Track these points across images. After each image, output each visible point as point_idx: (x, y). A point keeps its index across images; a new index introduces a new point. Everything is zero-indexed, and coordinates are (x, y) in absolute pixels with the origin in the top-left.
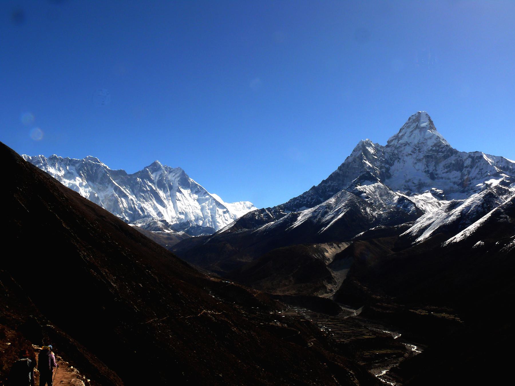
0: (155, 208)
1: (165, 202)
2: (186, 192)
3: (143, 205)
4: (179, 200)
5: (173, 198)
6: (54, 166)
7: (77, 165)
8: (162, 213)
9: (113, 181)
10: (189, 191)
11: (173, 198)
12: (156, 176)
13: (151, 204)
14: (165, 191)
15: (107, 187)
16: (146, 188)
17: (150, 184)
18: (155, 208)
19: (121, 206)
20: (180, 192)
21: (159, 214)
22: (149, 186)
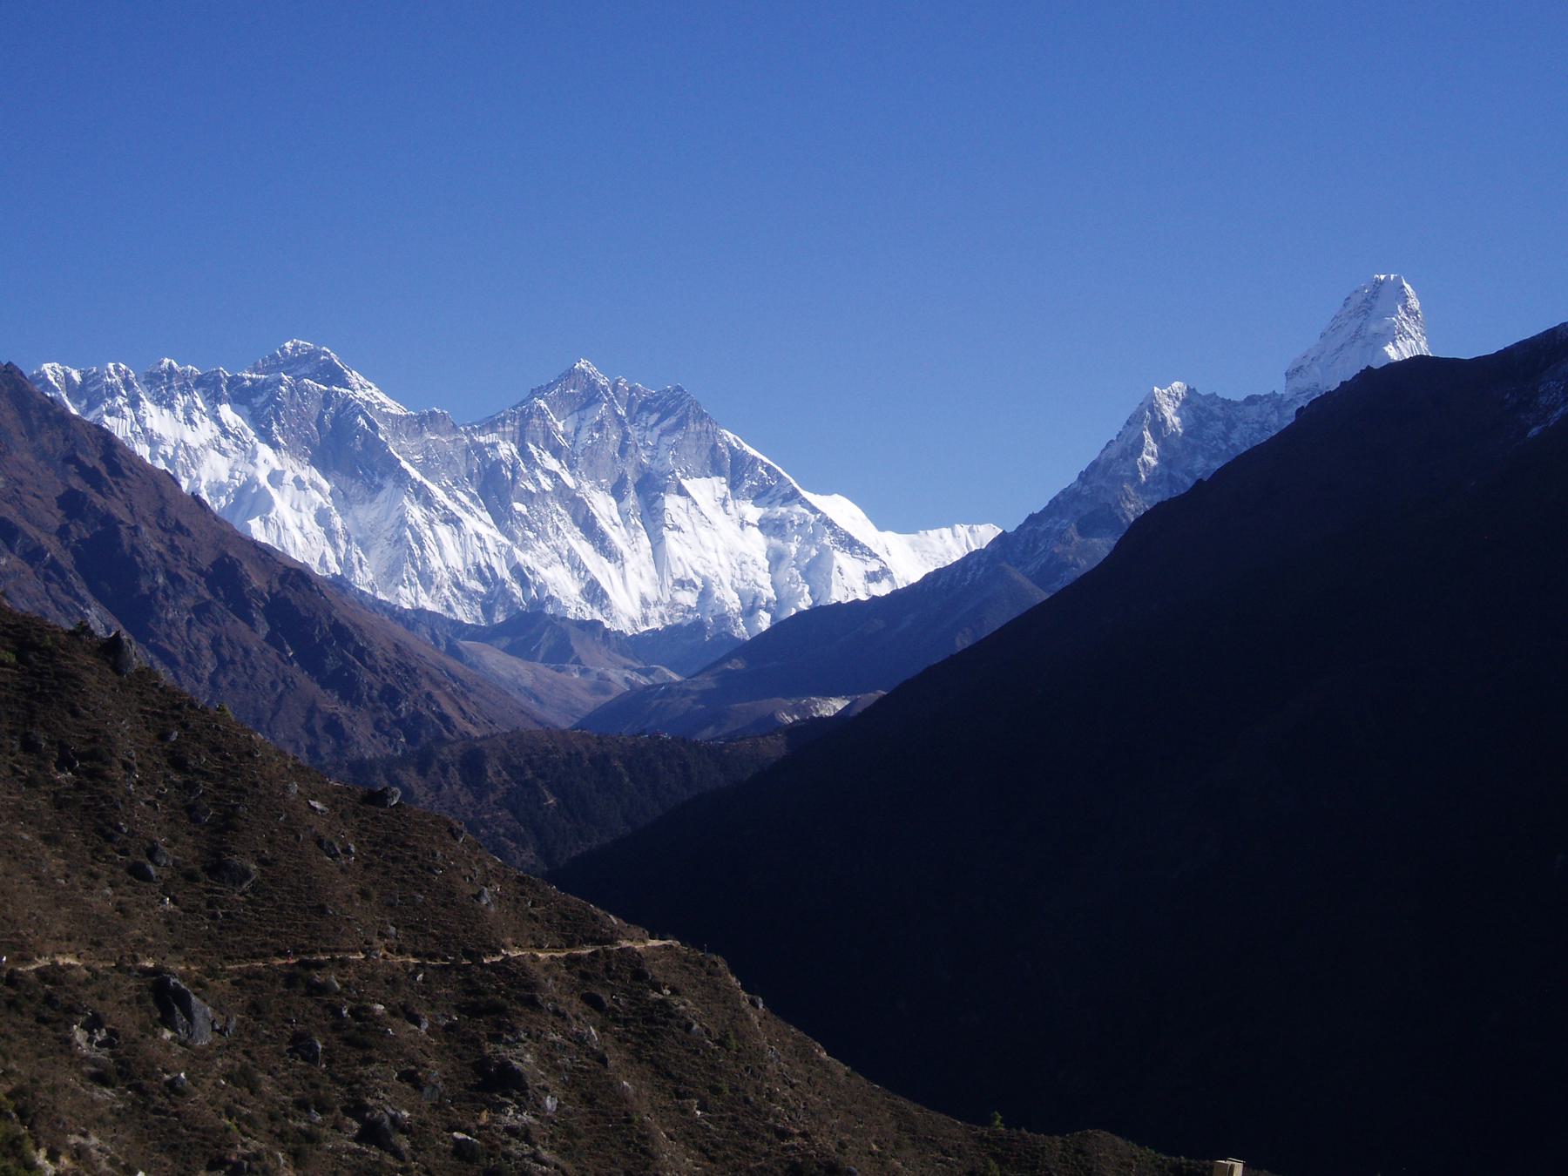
0: (577, 566)
1: (617, 537)
2: (706, 489)
3: (522, 557)
4: (678, 528)
5: (652, 518)
6: (171, 407)
7: (259, 401)
8: (604, 584)
9: (404, 464)
10: (719, 485)
11: (652, 518)
12: (577, 430)
13: (555, 549)
14: (618, 492)
15: (380, 488)
16: (538, 483)
17: (553, 464)
18: (577, 566)
19: (436, 563)
20: (682, 491)
21: (594, 593)
22: (548, 473)
